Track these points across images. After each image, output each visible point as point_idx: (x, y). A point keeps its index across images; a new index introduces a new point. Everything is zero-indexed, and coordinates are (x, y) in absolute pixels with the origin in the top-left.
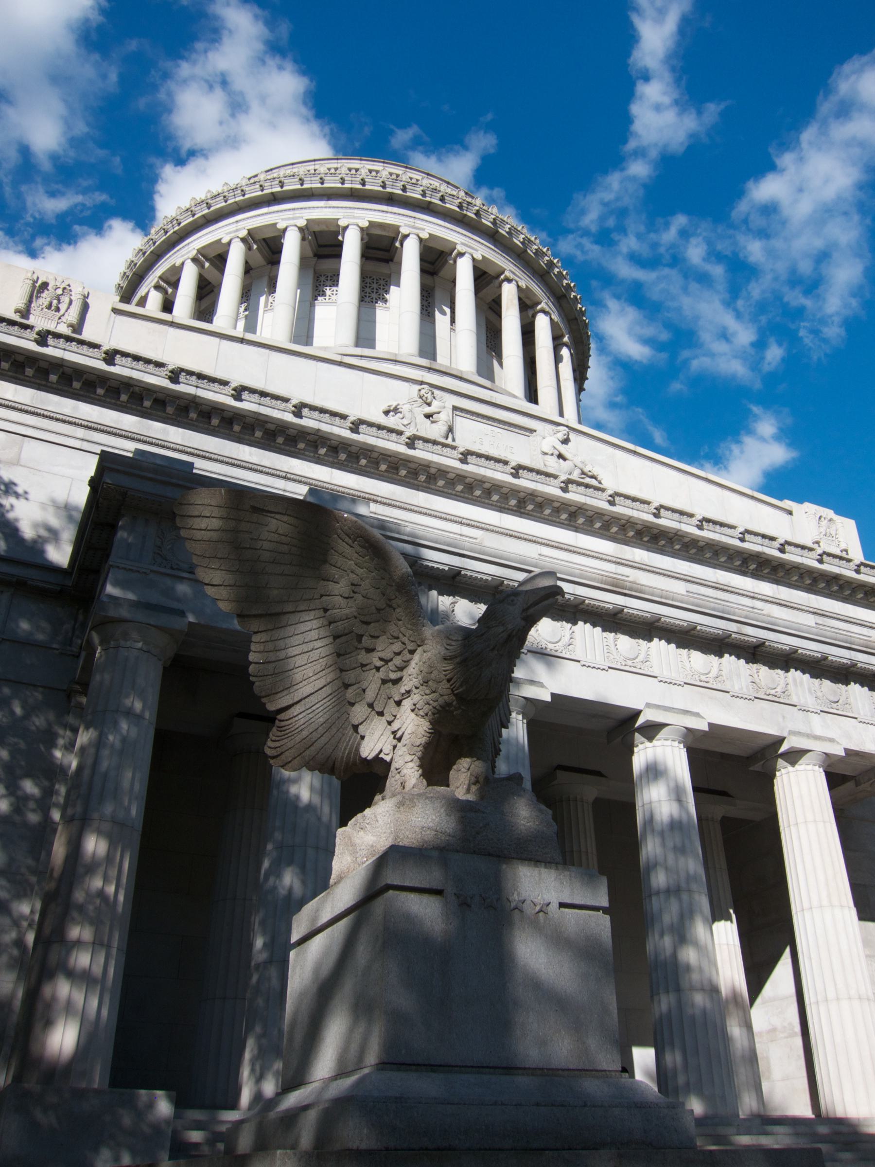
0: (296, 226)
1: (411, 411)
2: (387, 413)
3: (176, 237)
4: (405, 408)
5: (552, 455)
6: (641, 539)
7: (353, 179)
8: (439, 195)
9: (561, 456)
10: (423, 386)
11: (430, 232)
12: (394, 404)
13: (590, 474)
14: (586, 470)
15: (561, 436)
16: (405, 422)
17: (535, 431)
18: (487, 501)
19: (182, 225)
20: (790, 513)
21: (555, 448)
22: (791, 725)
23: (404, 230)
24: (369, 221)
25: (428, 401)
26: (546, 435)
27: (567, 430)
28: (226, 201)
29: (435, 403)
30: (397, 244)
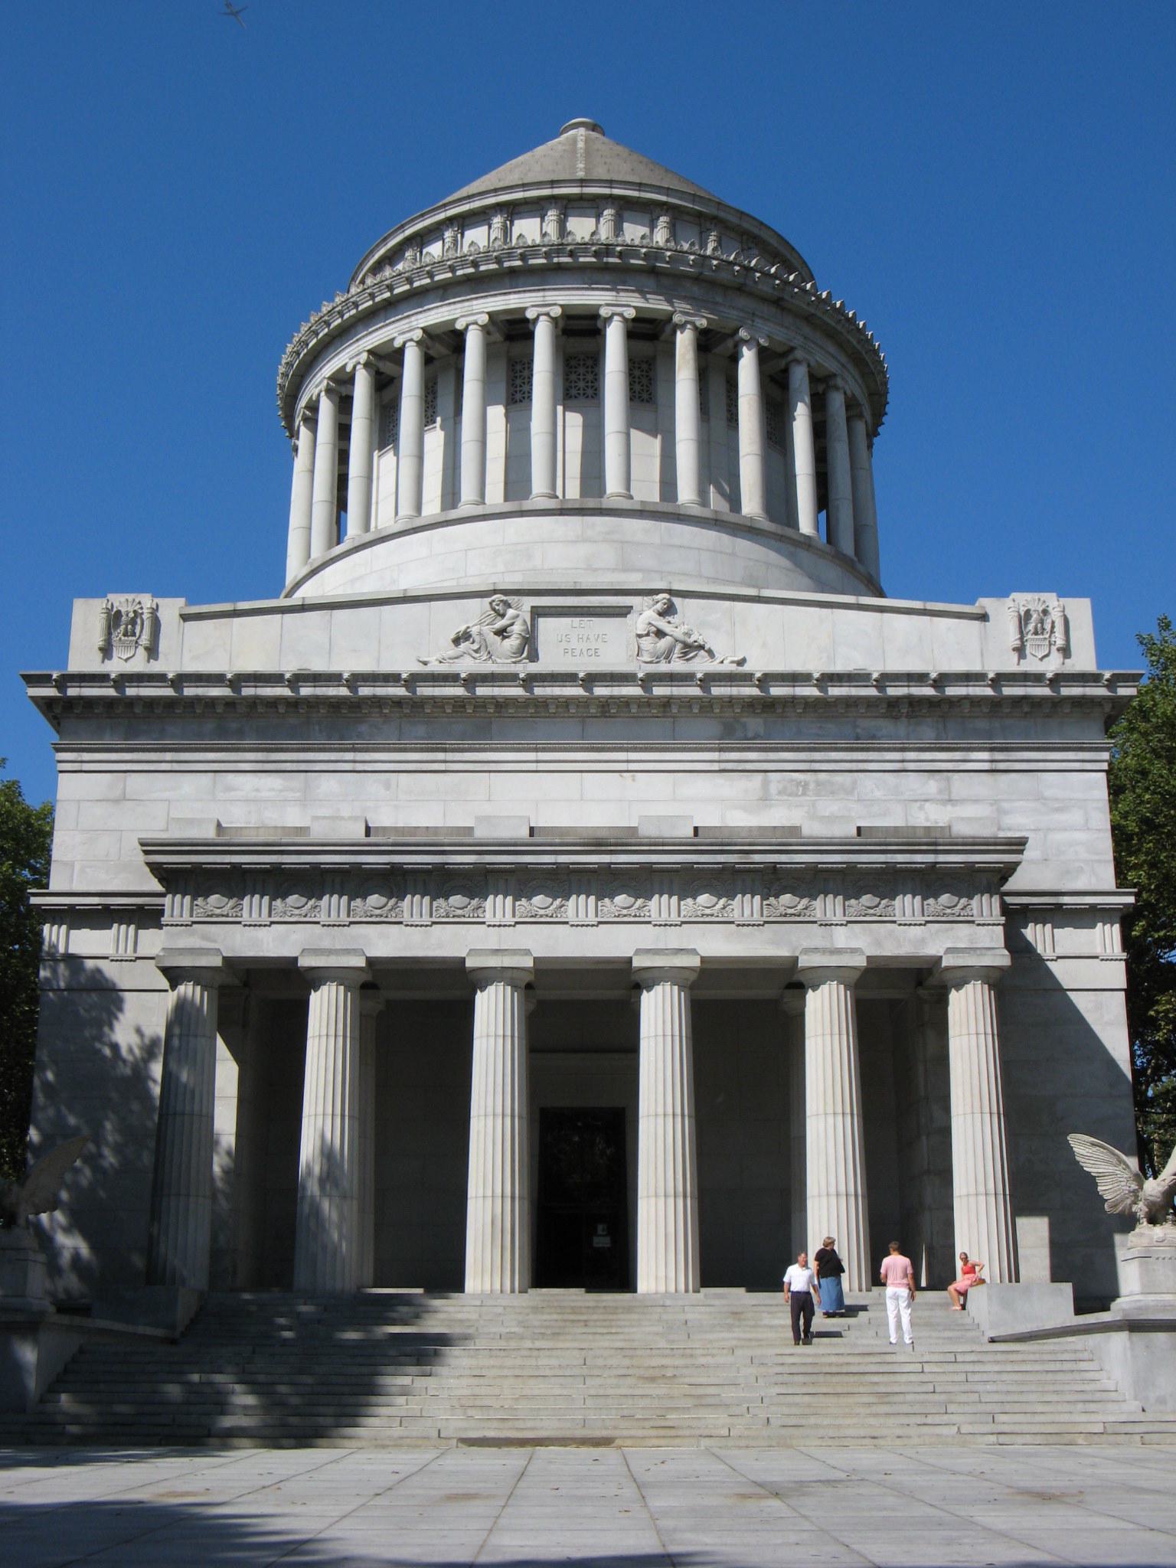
0: (411, 340)
1: (480, 634)
2: (457, 641)
4: (474, 631)
5: (648, 635)
6: (754, 712)
9: (660, 634)
10: (494, 597)
12: (463, 628)
14: (690, 640)
15: (659, 606)
16: (476, 646)
17: (632, 607)
19: (310, 345)
20: (983, 617)
22: (805, 944)
23: (530, 314)
24: (488, 313)
25: (501, 612)
26: (645, 608)
27: (666, 596)
28: (342, 317)
30: (531, 326)
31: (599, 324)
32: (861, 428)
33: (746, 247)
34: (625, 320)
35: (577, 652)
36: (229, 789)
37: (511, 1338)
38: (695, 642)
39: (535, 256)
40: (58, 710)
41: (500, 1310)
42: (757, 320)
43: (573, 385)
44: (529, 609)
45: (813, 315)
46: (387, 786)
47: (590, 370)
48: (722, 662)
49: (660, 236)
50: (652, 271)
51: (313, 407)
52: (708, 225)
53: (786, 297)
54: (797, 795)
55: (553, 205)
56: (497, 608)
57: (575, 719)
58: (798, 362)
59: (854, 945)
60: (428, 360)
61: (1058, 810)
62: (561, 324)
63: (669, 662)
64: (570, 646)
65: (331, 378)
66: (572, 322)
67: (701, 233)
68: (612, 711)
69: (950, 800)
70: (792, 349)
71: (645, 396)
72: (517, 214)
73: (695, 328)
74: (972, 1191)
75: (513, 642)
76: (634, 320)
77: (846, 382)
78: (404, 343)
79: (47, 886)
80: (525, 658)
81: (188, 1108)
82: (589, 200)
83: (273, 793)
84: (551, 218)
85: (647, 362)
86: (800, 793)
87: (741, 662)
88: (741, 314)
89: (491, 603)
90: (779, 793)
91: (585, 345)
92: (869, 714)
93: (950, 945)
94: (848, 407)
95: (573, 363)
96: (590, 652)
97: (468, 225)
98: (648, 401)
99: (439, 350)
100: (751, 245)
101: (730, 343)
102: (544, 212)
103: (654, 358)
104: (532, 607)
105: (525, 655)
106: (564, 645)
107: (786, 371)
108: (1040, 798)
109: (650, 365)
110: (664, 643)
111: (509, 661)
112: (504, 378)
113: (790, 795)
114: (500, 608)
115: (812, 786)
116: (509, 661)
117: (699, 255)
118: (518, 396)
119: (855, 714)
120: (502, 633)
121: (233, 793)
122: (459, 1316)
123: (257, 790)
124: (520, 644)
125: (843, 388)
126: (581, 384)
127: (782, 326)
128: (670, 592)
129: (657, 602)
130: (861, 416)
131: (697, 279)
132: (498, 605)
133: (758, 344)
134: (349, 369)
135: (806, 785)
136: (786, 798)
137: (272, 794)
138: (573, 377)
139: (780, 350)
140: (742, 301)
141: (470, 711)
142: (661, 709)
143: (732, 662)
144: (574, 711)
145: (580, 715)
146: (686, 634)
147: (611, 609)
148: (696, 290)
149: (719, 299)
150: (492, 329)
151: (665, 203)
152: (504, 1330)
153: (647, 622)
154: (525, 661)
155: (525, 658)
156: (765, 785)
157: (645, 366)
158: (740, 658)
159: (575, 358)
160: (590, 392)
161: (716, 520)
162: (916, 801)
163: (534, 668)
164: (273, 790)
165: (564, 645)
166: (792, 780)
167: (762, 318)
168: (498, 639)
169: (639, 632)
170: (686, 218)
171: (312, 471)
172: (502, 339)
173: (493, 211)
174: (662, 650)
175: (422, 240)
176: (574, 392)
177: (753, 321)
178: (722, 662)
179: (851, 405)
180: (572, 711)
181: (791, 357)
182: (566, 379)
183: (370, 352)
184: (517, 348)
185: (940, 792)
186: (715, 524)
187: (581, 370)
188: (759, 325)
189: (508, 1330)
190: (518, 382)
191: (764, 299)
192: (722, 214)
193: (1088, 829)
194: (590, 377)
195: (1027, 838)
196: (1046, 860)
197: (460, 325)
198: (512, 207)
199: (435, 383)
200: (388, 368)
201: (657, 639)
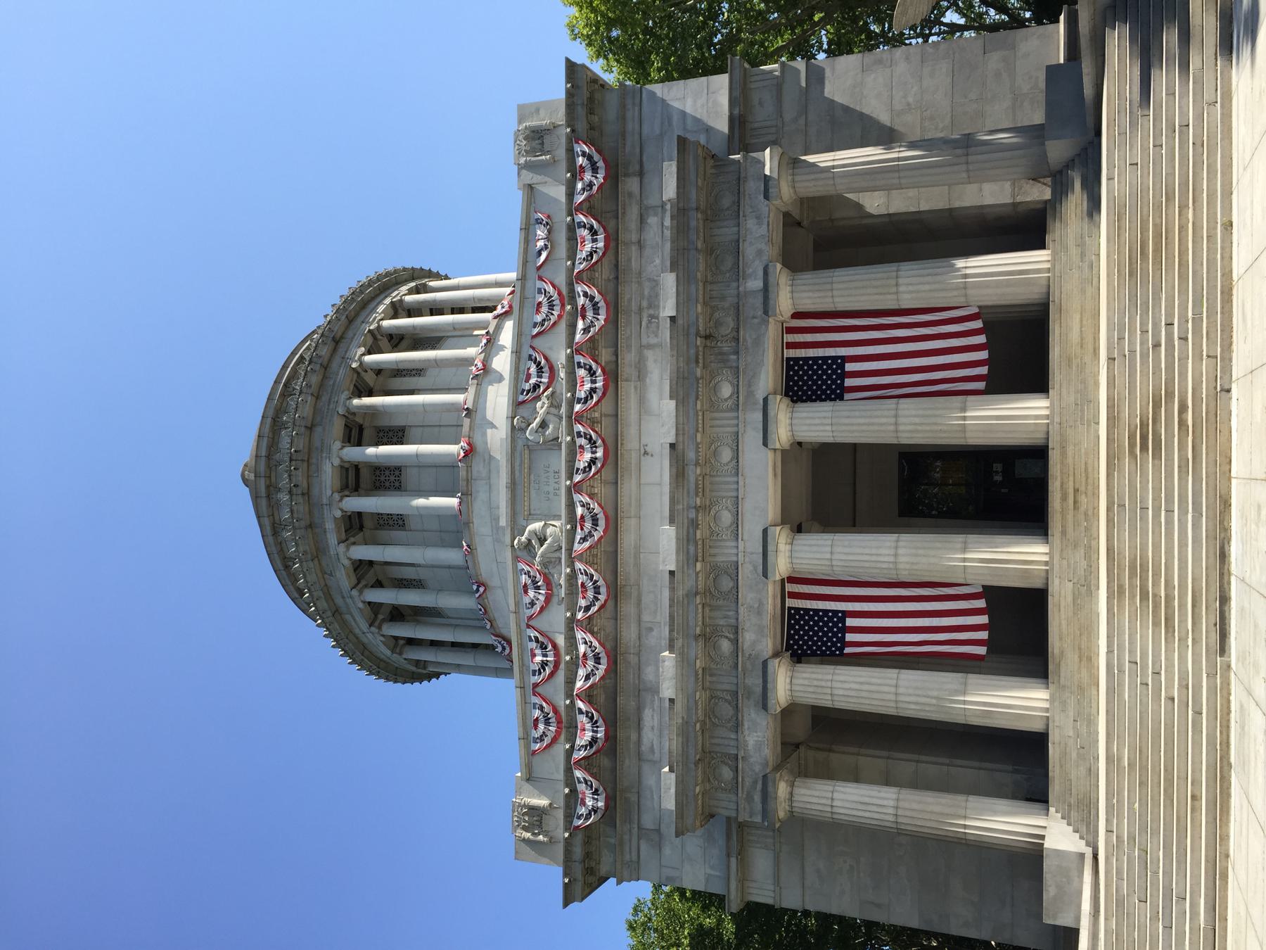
3: (382, 665)
8: (294, 489)
9: (543, 425)
18: (599, 495)
21: (536, 432)
23: (338, 514)
31: (346, 465)
32: (434, 284)
34: (343, 447)
35: (557, 486)
36: (652, 750)
37: (1090, 557)
40: (591, 879)
41: (1065, 562)
42: (346, 357)
43: (382, 484)
45: (347, 317)
46: (651, 629)
51: (417, 663)
54: (658, 323)
57: (603, 489)
59: (761, 273)
60: (379, 584)
61: (670, 124)
65: (393, 652)
66: (350, 486)
69: (662, 207)
71: (400, 434)
74: (964, 167)
77: (398, 294)
78: (364, 602)
79: (724, 896)
81: (891, 811)
83: (655, 715)
86: (657, 321)
88: (343, 365)
90: (656, 336)
92: (600, 270)
93: (762, 196)
94: (418, 292)
99: (371, 577)
103: (374, 427)
108: (662, 135)
113: (658, 328)
115: (651, 312)
118: (400, 522)
119: (600, 280)
120: (542, 541)
121: (655, 746)
122: (1070, 599)
123: (653, 728)
125: (401, 297)
126: (392, 478)
127: (353, 338)
130: (425, 285)
133: (363, 355)
134: (382, 639)
135: (652, 317)
136: (660, 331)
137: (655, 718)
138: (387, 484)
140: (334, 365)
142: (595, 425)
145: (599, 485)
148: (325, 398)
149: (331, 383)
150: (352, 540)
152: (1084, 564)
156: (650, 347)
157: (381, 434)
160: (397, 473)
162: (663, 232)
164: (653, 716)
165: (551, 496)
166: (647, 327)
167: (346, 352)
168: (544, 546)
171: (459, 665)
172: (362, 533)
176: (397, 484)
177: (348, 358)
179: (417, 290)
180: (596, 492)
181: (376, 333)
182: (387, 489)
183: (370, 626)
184: (368, 523)
185: (656, 215)
187: (382, 478)
189: (1083, 560)
190: (391, 522)
191: (335, 350)
193: (684, 98)
194: (387, 473)
195: (678, 136)
196: (707, 130)
197: (347, 562)
199: (396, 579)
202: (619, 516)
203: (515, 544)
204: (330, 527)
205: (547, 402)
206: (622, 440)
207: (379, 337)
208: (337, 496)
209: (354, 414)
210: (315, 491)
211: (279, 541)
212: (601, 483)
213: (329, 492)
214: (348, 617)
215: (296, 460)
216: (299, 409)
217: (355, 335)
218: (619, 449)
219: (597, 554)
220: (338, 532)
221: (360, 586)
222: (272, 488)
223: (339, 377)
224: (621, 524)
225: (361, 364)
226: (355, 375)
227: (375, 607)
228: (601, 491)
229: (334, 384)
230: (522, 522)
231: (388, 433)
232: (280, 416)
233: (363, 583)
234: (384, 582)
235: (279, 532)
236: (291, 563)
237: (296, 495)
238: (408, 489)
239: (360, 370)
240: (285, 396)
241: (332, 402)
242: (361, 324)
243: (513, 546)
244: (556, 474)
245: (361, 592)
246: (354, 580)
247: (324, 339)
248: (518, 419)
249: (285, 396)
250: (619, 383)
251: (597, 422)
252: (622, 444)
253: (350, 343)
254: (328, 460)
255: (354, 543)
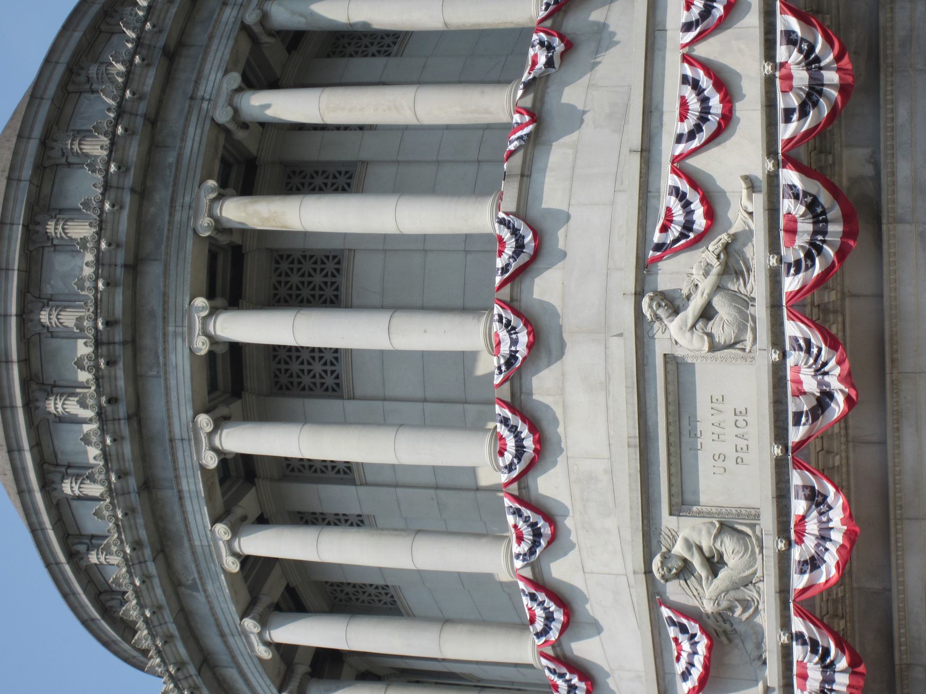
1: (716, 600)
7: (136, 561)
8: (109, 409)
9: (707, 313)
10: (658, 576)
11: (190, 413)
13: (722, 256)
14: (716, 267)
15: (661, 312)
17: (665, 355)
18: (844, 469)
21: (694, 326)
23: (211, 461)
24: (213, 523)
25: (680, 564)
27: (645, 302)
29: (679, 549)
30: (228, 457)
31: (220, 350)
33: (88, 87)
34: (214, 311)
35: (742, 443)
38: (718, 257)
39: (120, 457)
42: (200, 93)
44: (675, 518)
47: (295, 380)
48: (751, 214)
49: (81, 230)
50: (134, 267)
52: (56, 153)
53: (161, 41)
55: (38, 404)
56: (674, 571)
57: (851, 455)
58: (265, 17)
62: (223, 411)
63: (753, 299)
64: (732, 455)
67: (69, 165)
68: (837, 463)
70: (245, 28)
71: (330, 266)
72: (56, 457)
73: (221, 197)
75: (728, 546)
76: (210, 296)
78: (268, 644)
80: (754, 532)
82: (28, 351)
84: (59, 405)
85: (277, 262)
87: (751, 184)
88: (194, 119)
89: (667, 581)
91: (255, 375)
95: (284, 379)
96: (741, 423)
97: (78, 529)
98: (339, 263)
100: (82, 78)
101: (240, 135)
102: (51, 418)
103: (271, 250)
104: (671, 514)
105: (748, 530)
106: (730, 464)
107: (281, 34)
109: (281, 257)
110: (719, 303)
111: (759, 557)
112: (314, 486)
114: (675, 565)
116: (759, 557)
117: (103, 194)
120: (714, 564)
124: (732, 536)
127: (208, 47)
128: (639, 295)
129: (656, 315)
131: (142, 193)
132: (670, 570)
138: (307, 380)
139: (245, 46)
140: (174, 115)
141: (842, 623)
142: (831, 317)
143: (750, 198)
144: (837, 458)
145: (843, 447)
146: (706, 274)
147: (671, 388)
148: (161, 195)
149: (171, 158)
151: (26, 227)
153: (688, 334)
154: (758, 532)
155: (754, 532)
157: (284, 266)
158: (744, 185)
159: (276, 376)
161: (522, 175)
163: (768, 521)
165: (730, 464)
167: (197, 83)
168: (723, 574)
169: (706, 348)
170: (46, 190)
173: (55, 494)
174: (734, 313)
175: (106, 592)
176: (329, 381)
177: (203, 99)
178: (751, 214)
181: (257, 29)
186: (529, 176)
187: (295, 367)
188: (209, 89)
191: (167, 80)
192: (37, 131)
197: (233, 566)
198: (46, 466)
199: (327, 582)
200: (302, 668)
201: (717, 319)
202: (892, 516)
203: (655, 569)
204: (193, 487)
205: (715, 263)
206: (894, 352)
207: (265, 39)
208: (204, 421)
209: (229, 231)
210: (156, 407)
211: (55, 502)
212: (847, 441)
213: (187, 412)
214: (232, 673)
215: (109, 343)
216: (108, 226)
217: (211, 38)
218: (888, 370)
219: (843, 597)
220: (210, 499)
221: (259, 608)
222: (34, 386)
223: (189, 144)
224: (897, 533)
225: (236, 111)
226: (222, 142)
227: (286, 652)
228: (847, 458)
229: (178, 162)
230: (668, 522)
231: (300, 262)
232: (39, 218)
233: (266, 600)
234: (307, 595)
235: (53, 482)
236: (82, 548)
237: (114, 420)
238: (358, 392)
239: (232, 127)
240: (45, 168)
241: (178, 208)
242: (221, 9)
243: (648, 572)
244: (740, 418)
245: (264, 623)
246: (245, 596)
247: (144, 52)
248: (652, 299)
249: (45, 168)
250: (884, 227)
251: (835, 312)
252: (893, 361)
253: (204, 59)
254: (179, 341)
255: (244, 519)
